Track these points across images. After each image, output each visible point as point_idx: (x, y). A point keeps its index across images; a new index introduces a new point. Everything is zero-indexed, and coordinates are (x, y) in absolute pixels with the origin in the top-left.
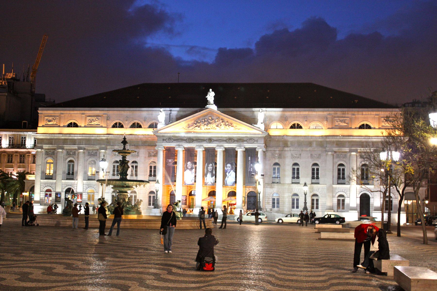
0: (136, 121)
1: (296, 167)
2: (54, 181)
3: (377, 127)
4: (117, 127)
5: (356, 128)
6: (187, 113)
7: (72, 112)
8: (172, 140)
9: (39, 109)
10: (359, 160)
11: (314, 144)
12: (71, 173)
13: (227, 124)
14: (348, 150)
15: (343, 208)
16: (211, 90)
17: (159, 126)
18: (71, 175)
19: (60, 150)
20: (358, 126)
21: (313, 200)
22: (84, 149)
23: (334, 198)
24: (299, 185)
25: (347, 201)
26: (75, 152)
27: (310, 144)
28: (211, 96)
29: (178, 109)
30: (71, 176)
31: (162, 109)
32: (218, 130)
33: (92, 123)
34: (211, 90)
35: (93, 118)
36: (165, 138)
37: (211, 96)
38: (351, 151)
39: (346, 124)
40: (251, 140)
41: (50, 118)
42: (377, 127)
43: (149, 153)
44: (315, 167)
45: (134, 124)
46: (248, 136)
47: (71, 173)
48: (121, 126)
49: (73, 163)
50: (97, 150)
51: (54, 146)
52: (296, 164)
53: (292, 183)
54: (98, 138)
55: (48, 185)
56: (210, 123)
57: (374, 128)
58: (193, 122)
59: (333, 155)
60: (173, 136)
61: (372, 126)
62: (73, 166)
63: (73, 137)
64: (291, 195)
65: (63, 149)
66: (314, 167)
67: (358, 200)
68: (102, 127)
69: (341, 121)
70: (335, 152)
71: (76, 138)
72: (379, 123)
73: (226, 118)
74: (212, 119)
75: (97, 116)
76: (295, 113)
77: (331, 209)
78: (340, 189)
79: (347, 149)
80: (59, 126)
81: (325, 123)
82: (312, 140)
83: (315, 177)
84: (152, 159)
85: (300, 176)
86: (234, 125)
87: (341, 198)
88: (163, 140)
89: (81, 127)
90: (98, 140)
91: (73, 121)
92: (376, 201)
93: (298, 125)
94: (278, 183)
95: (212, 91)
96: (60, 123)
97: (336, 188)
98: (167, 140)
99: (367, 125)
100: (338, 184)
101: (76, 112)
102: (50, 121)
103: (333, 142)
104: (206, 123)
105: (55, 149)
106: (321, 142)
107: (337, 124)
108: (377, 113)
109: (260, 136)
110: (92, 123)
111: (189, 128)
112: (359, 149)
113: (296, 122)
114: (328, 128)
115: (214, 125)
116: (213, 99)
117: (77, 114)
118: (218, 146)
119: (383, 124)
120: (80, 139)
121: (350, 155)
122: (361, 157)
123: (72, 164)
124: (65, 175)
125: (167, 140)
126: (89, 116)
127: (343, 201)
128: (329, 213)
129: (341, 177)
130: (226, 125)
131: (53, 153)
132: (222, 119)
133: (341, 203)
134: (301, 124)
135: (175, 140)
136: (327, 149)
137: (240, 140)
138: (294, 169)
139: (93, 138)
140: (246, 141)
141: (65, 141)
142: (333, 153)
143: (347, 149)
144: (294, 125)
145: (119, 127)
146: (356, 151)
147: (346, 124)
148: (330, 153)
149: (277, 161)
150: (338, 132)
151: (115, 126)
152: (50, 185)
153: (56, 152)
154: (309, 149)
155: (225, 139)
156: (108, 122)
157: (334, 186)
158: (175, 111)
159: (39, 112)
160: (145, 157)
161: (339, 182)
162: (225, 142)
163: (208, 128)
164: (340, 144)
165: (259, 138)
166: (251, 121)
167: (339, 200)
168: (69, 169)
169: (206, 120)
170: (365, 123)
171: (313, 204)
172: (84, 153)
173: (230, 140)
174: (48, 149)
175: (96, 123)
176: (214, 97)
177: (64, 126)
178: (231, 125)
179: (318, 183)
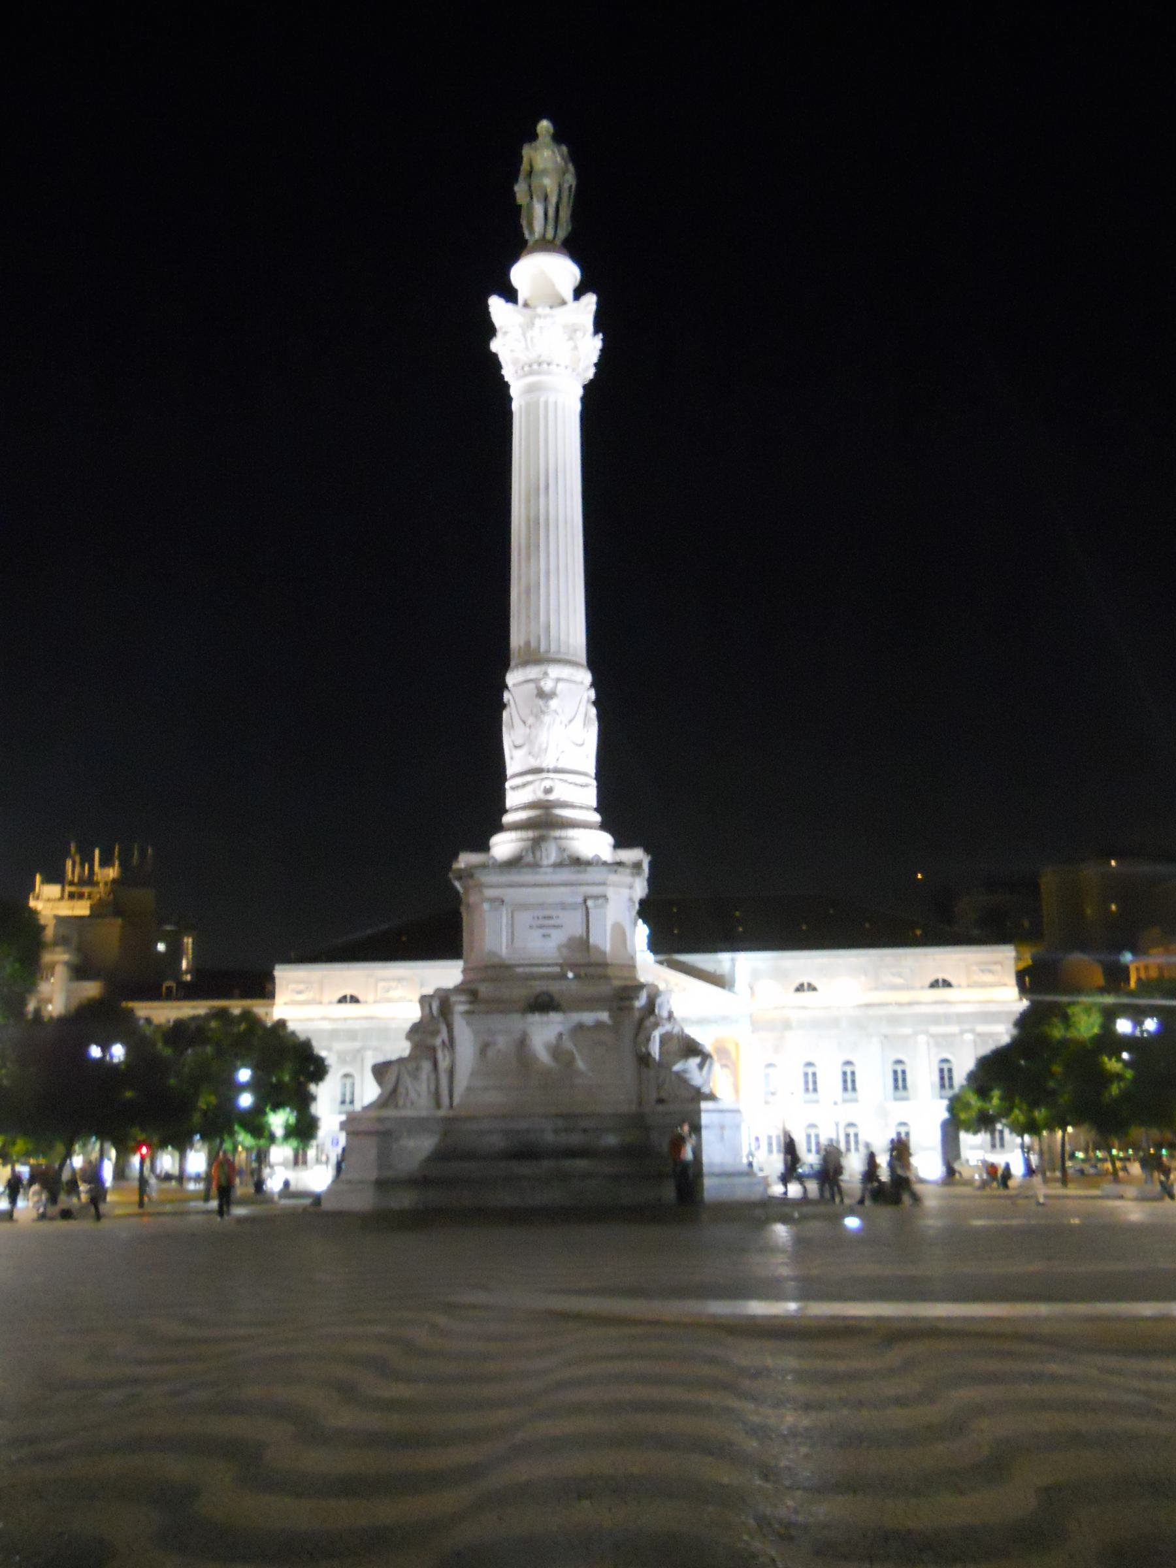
21: (848, 1135)
27: (835, 1022)
41: (301, 987)
57: (959, 986)
62: (353, 1085)
69: (893, 975)
70: (886, 1037)
75: (400, 980)
79: (907, 1030)
91: (348, 992)
93: (809, 985)
100: (896, 1099)
102: (300, 992)
112: (934, 1029)
113: (805, 980)
122: (937, 1044)
123: (348, 1081)
126: (384, 980)
134: (815, 983)
143: (907, 1030)
144: (802, 985)
164: (894, 1020)
168: (344, 1095)
171: (848, 1142)
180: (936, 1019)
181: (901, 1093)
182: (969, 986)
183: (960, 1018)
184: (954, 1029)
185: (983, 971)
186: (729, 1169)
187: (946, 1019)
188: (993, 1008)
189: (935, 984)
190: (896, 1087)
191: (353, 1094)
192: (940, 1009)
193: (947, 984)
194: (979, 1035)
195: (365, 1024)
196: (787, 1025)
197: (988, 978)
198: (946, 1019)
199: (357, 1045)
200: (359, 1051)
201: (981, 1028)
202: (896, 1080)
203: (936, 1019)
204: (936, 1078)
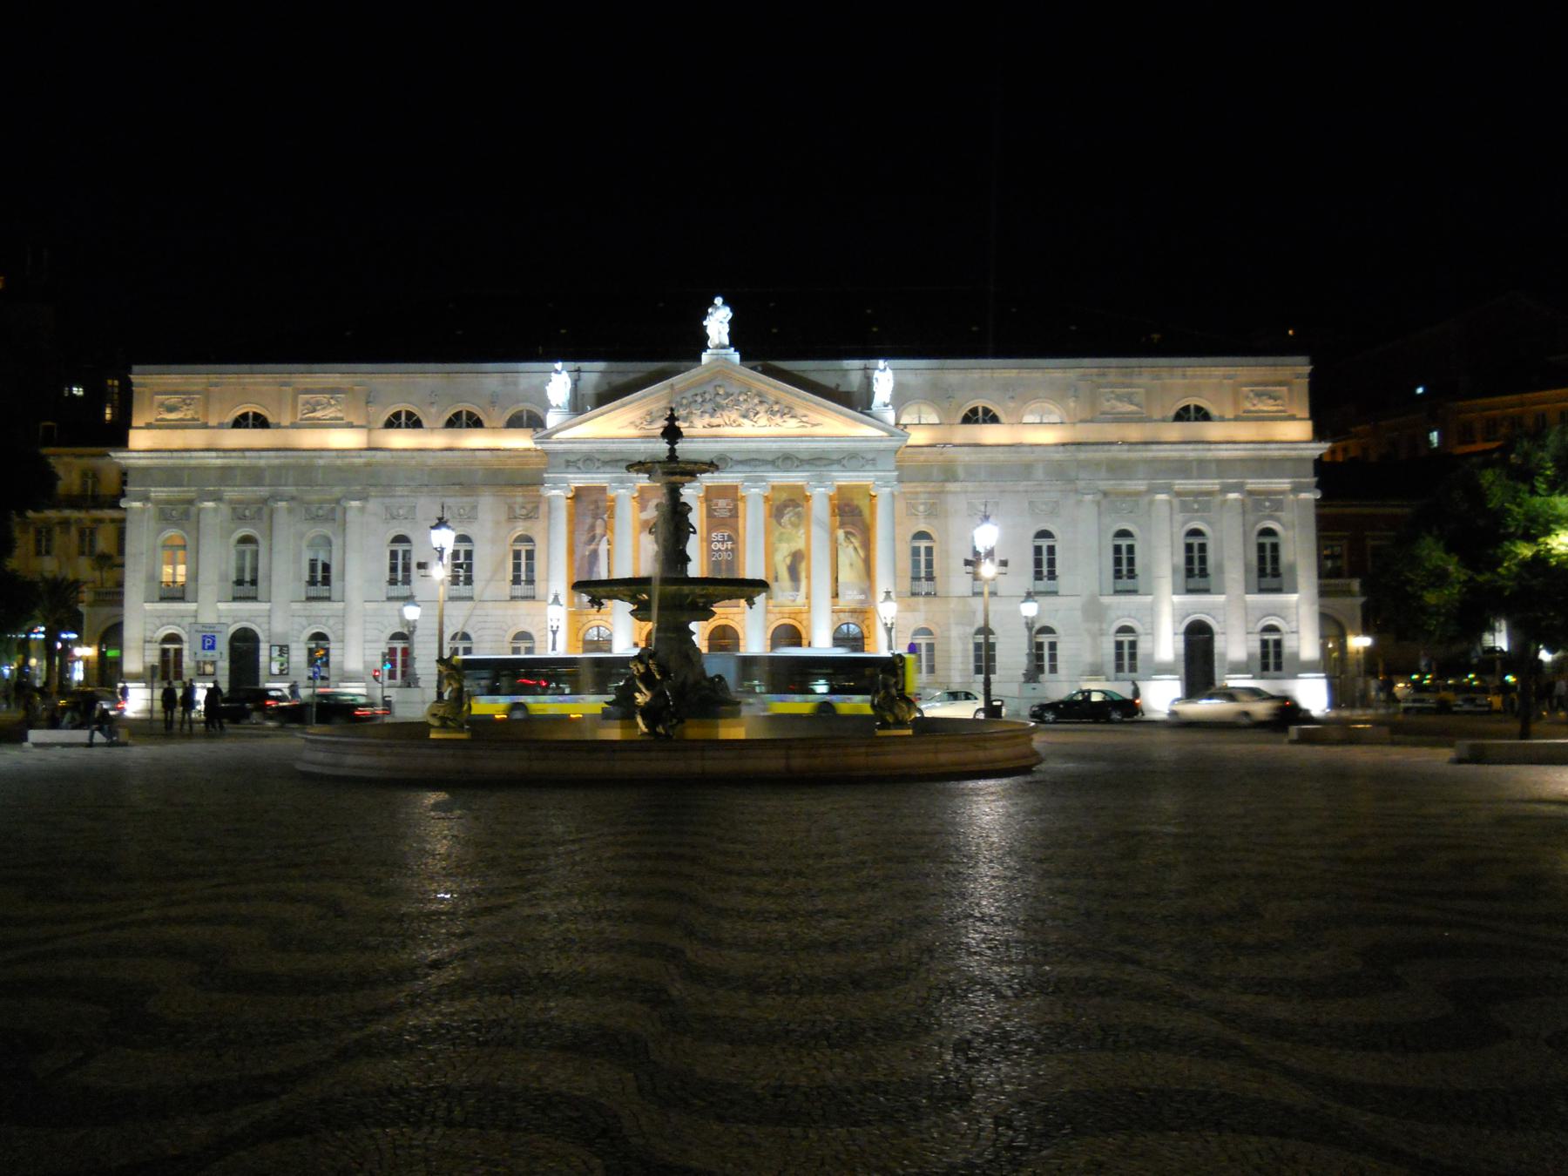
0: (464, 407)
2: (192, 606)
3: (1229, 414)
4: (399, 426)
5: (1164, 420)
6: (632, 376)
7: (247, 379)
9: (136, 368)
10: (1179, 517)
11: (1039, 473)
12: (248, 578)
13: (776, 408)
14: (1143, 488)
15: (1278, 667)
16: (718, 301)
17: (552, 420)
18: (247, 586)
19: (210, 504)
20: (1172, 413)
23: (1104, 639)
25: (1142, 648)
26: (333, 510)
27: (1026, 470)
28: (718, 322)
29: (600, 365)
30: (246, 589)
31: (559, 366)
32: (747, 428)
33: (318, 414)
34: (718, 301)
35: (319, 397)
36: (572, 458)
37: (718, 322)
38: (1152, 490)
39: (1133, 408)
40: (852, 457)
41: (174, 400)
42: (1229, 414)
43: (511, 508)
44: (1045, 543)
45: (458, 415)
46: (845, 445)
47: (248, 578)
48: (414, 422)
49: (253, 547)
50: (338, 501)
51: (190, 492)
54: (339, 462)
56: (722, 408)
57: (1222, 419)
59: (1098, 504)
60: (598, 451)
61: (1213, 411)
62: (256, 555)
63: (254, 462)
64: (973, 630)
65: (218, 498)
66: (1191, 540)
67: (1181, 639)
68: (350, 426)
69: (1119, 398)
70: (1105, 494)
71: (262, 462)
72: (1236, 403)
73: (772, 391)
74: (728, 395)
75: (334, 391)
76: (976, 375)
77: (1096, 671)
78: (1123, 609)
79: (1140, 485)
80: (205, 426)
81: (1072, 405)
82: (1031, 457)
84: (520, 529)
86: (800, 411)
87: (1126, 638)
88: (568, 463)
89: (278, 426)
90: (339, 469)
91: (250, 408)
92: (1234, 645)
93: (986, 411)
94: (928, 594)
96: (206, 415)
97: (1108, 607)
98: (580, 464)
99: (1198, 409)
100: (1117, 592)
101: (260, 378)
102: (171, 409)
103: (1098, 464)
104: (708, 406)
105: (191, 502)
106: (1060, 463)
107: (1106, 406)
108: (1231, 371)
109: (882, 445)
110: (318, 414)
111: (651, 423)
112: (1180, 484)
113: (980, 403)
114: (1082, 421)
115: (734, 415)
117: (264, 384)
118: (747, 479)
119: (1248, 406)
120: (279, 468)
121: (1151, 503)
122: (1185, 508)
123: (249, 548)
124: (229, 588)
125: (580, 464)
126: (307, 391)
127: (1133, 645)
128: (1086, 686)
129: (1196, 569)
130: (773, 413)
131: (186, 514)
132: (759, 394)
133: (1127, 655)
134: (996, 409)
135: (605, 463)
136: (1081, 484)
137: (819, 460)
139: (321, 462)
140: (839, 461)
141: (225, 475)
142: (1099, 497)
143: (1140, 485)
144: (974, 411)
145: (407, 426)
146: (1167, 489)
147: (1133, 408)
148: (1090, 497)
149: (922, 527)
150: (1111, 432)
151: (393, 423)
153: (193, 510)
154: (1022, 485)
155: (770, 458)
156: (372, 409)
157: (1106, 600)
158: (594, 371)
159: (134, 378)
160: (498, 523)
161: (1264, 586)
162: (769, 467)
163: (715, 421)
164: (1119, 469)
165: (879, 451)
166: (857, 401)
167: (1119, 645)
168: (241, 570)
169: (708, 397)
170: (1193, 401)
173: (786, 460)
174: (168, 502)
175: (330, 413)
176: (731, 322)
177: (221, 426)
178: (788, 411)
180: (1183, 468)
181: (1125, 583)
182: (1237, 419)
183: (1223, 467)
184: (1212, 484)
185: (1259, 395)
186: (1526, 797)
187: (1201, 468)
188: (1274, 452)
189: (1183, 415)
190: (1118, 574)
191: (255, 570)
192: (1191, 453)
193: (1203, 415)
194: (1251, 493)
195: (274, 460)
196: (949, 473)
197: (1267, 406)
198: (1201, 468)
199: (263, 491)
200: (265, 501)
201: (1253, 484)
202: (1118, 562)
203: (1183, 468)
204: (1181, 559)
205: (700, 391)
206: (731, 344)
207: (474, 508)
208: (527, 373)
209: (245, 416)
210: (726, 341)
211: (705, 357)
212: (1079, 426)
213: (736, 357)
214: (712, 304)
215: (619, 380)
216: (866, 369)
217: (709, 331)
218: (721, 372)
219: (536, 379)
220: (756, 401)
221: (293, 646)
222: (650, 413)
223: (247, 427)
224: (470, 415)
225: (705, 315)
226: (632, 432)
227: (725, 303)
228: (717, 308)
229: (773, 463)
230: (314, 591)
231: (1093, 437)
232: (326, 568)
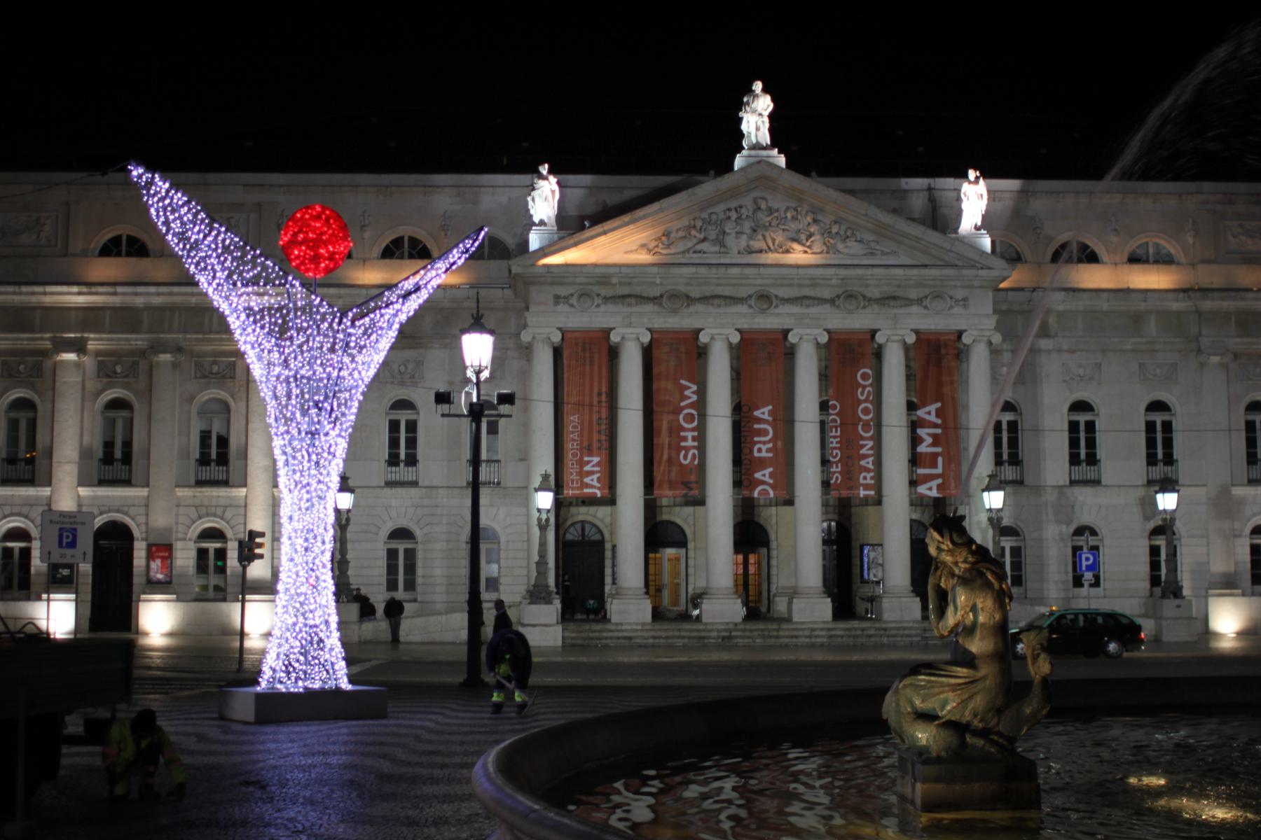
0: (406, 231)
1: (1082, 418)
8: (598, 301)
11: (1152, 327)
12: (118, 454)
16: (758, 86)
18: (118, 466)
19: (71, 356)
22: (179, 350)
23: (1238, 541)
24: (1098, 488)
27: (1137, 320)
30: (118, 469)
34: (758, 86)
36: (563, 291)
44: (1158, 418)
45: (398, 242)
47: (118, 454)
49: (125, 413)
52: (1080, 406)
53: (1073, 483)
55: (16, 510)
56: (768, 227)
58: (685, 222)
59: (1225, 366)
62: (129, 424)
63: (129, 300)
64: (1071, 530)
65: (79, 347)
70: (1236, 356)
71: (139, 301)
81: (1191, 240)
82: (1143, 306)
83: (1083, 456)
85: (1177, 452)
95: (765, 90)
97: (1242, 502)
105: (43, 353)
106: (1178, 314)
116: (765, 125)
120: (160, 309)
123: (121, 414)
125: (574, 301)
131: (38, 370)
138: (1073, 427)
148: (1215, 359)
152: (25, 510)
153: (48, 364)
157: (1238, 491)
162: (828, 306)
172: (175, 365)
176: (771, 116)
179: (1097, 482)
199: (138, 341)
200: (142, 353)
205: (733, 204)
206: (774, 144)
207: (419, 364)
208: (494, 188)
209: (116, 241)
210: (765, 138)
211: (739, 162)
212: (1201, 267)
213: (782, 161)
214: (749, 91)
215: (614, 199)
216: (930, 189)
217: (744, 127)
218: (761, 176)
219: (502, 197)
220: (809, 219)
221: (178, 545)
222: (667, 234)
223: (119, 254)
224: (414, 242)
225: (740, 105)
226: (643, 257)
227: (765, 90)
228: (757, 96)
229: (832, 301)
230: (206, 473)
231: (1217, 282)
232: (223, 442)
